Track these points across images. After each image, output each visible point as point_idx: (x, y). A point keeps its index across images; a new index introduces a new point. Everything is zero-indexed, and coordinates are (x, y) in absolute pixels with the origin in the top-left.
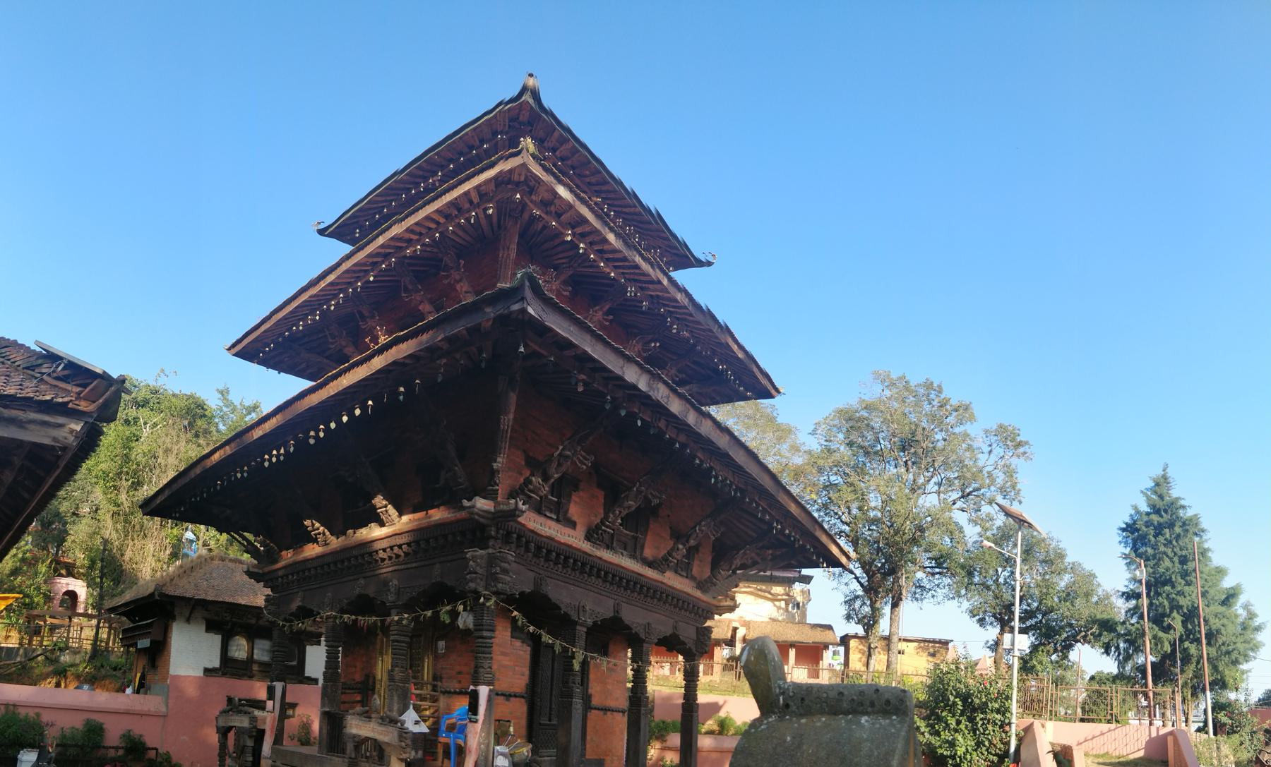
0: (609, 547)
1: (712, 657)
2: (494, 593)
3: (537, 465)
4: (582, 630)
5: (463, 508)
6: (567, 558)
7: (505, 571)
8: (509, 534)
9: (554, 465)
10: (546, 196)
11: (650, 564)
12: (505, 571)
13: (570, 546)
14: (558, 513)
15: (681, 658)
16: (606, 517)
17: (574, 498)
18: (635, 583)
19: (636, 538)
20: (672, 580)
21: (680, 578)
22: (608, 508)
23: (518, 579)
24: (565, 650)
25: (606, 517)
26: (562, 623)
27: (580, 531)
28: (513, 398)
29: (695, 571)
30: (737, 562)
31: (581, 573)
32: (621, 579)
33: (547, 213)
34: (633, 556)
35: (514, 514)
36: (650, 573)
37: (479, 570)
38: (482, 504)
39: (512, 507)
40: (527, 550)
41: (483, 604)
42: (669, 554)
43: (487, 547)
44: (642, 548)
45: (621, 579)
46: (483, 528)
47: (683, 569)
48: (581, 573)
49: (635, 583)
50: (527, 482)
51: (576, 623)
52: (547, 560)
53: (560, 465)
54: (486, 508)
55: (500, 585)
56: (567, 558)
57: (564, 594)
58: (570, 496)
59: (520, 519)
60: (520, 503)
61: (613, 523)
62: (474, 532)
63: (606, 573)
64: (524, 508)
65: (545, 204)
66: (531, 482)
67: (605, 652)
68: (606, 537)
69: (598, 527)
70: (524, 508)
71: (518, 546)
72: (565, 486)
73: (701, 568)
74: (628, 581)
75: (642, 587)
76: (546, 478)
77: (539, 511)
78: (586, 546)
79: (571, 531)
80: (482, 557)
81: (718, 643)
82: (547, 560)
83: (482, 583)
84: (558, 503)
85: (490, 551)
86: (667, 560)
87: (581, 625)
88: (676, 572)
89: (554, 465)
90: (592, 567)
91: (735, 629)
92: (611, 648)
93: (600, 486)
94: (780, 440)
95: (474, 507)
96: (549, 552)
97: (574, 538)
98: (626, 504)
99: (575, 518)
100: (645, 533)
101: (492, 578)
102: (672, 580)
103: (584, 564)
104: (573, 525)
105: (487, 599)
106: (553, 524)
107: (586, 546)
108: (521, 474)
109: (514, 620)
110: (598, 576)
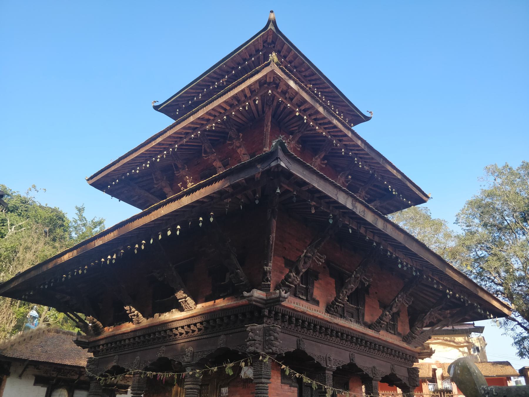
0: (342, 316)
1: (421, 390)
2: (268, 353)
3: (291, 264)
4: (329, 373)
5: (244, 297)
6: (315, 325)
7: (276, 339)
8: (276, 314)
9: (302, 263)
10: (285, 88)
11: (370, 327)
12: (276, 339)
13: (316, 317)
14: (307, 296)
15: (399, 391)
16: (338, 296)
17: (316, 284)
18: (362, 340)
19: (358, 310)
20: (384, 336)
21: (390, 335)
22: (339, 290)
23: (285, 343)
24: (320, 387)
25: (338, 296)
26: (315, 369)
27: (322, 307)
28: (274, 223)
29: (400, 329)
30: (427, 321)
31: (326, 335)
32: (352, 337)
33: (286, 99)
34: (358, 322)
35: (278, 300)
36: (370, 332)
37: (257, 338)
38: (258, 294)
39: (278, 295)
40: (290, 322)
41: (262, 361)
42: (381, 318)
43: (263, 323)
45: (352, 337)
46: (260, 310)
47: (392, 328)
48: (326, 335)
49: (362, 340)
50: (288, 277)
51: (324, 369)
52: (303, 327)
53: (305, 263)
54: (262, 296)
56: (315, 325)
57: (316, 350)
58: (313, 283)
59: (283, 303)
60: (283, 293)
61: (343, 300)
62: (254, 313)
63: (342, 334)
64: (286, 295)
65: (284, 93)
66: (290, 277)
67: (346, 387)
68: (339, 309)
70: (286, 295)
71: (283, 322)
72: (310, 278)
73: (403, 327)
74: (357, 339)
75: (366, 342)
76: (297, 273)
77: (295, 295)
78: (327, 317)
79: (315, 307)
80: (259, 330)
81: (424, 380)
82: (303, 327)
83: (261, 347)
84: (307, 289)
85: (265, 325)
86: (380, 323)
87: (328, 370)
88: (387, 331)
89: (302, 263)
90: (332, 331)
91: (434, 370)
92: (351, 385)
93: (332, 275)
94: (437, 231)
95: (252, 296)
96: (303, 322)
97: (318, 312)
98: (349, 286)
99: (318, 298)
101: (267, 343)
102: (384, 336)
103: (327, 329)
104: (317, 303)
105: (264, 357)
106: (304, 303)
107: (327, 317)
108: (281, 272)
109: (283, 371)
110: (337, 336)
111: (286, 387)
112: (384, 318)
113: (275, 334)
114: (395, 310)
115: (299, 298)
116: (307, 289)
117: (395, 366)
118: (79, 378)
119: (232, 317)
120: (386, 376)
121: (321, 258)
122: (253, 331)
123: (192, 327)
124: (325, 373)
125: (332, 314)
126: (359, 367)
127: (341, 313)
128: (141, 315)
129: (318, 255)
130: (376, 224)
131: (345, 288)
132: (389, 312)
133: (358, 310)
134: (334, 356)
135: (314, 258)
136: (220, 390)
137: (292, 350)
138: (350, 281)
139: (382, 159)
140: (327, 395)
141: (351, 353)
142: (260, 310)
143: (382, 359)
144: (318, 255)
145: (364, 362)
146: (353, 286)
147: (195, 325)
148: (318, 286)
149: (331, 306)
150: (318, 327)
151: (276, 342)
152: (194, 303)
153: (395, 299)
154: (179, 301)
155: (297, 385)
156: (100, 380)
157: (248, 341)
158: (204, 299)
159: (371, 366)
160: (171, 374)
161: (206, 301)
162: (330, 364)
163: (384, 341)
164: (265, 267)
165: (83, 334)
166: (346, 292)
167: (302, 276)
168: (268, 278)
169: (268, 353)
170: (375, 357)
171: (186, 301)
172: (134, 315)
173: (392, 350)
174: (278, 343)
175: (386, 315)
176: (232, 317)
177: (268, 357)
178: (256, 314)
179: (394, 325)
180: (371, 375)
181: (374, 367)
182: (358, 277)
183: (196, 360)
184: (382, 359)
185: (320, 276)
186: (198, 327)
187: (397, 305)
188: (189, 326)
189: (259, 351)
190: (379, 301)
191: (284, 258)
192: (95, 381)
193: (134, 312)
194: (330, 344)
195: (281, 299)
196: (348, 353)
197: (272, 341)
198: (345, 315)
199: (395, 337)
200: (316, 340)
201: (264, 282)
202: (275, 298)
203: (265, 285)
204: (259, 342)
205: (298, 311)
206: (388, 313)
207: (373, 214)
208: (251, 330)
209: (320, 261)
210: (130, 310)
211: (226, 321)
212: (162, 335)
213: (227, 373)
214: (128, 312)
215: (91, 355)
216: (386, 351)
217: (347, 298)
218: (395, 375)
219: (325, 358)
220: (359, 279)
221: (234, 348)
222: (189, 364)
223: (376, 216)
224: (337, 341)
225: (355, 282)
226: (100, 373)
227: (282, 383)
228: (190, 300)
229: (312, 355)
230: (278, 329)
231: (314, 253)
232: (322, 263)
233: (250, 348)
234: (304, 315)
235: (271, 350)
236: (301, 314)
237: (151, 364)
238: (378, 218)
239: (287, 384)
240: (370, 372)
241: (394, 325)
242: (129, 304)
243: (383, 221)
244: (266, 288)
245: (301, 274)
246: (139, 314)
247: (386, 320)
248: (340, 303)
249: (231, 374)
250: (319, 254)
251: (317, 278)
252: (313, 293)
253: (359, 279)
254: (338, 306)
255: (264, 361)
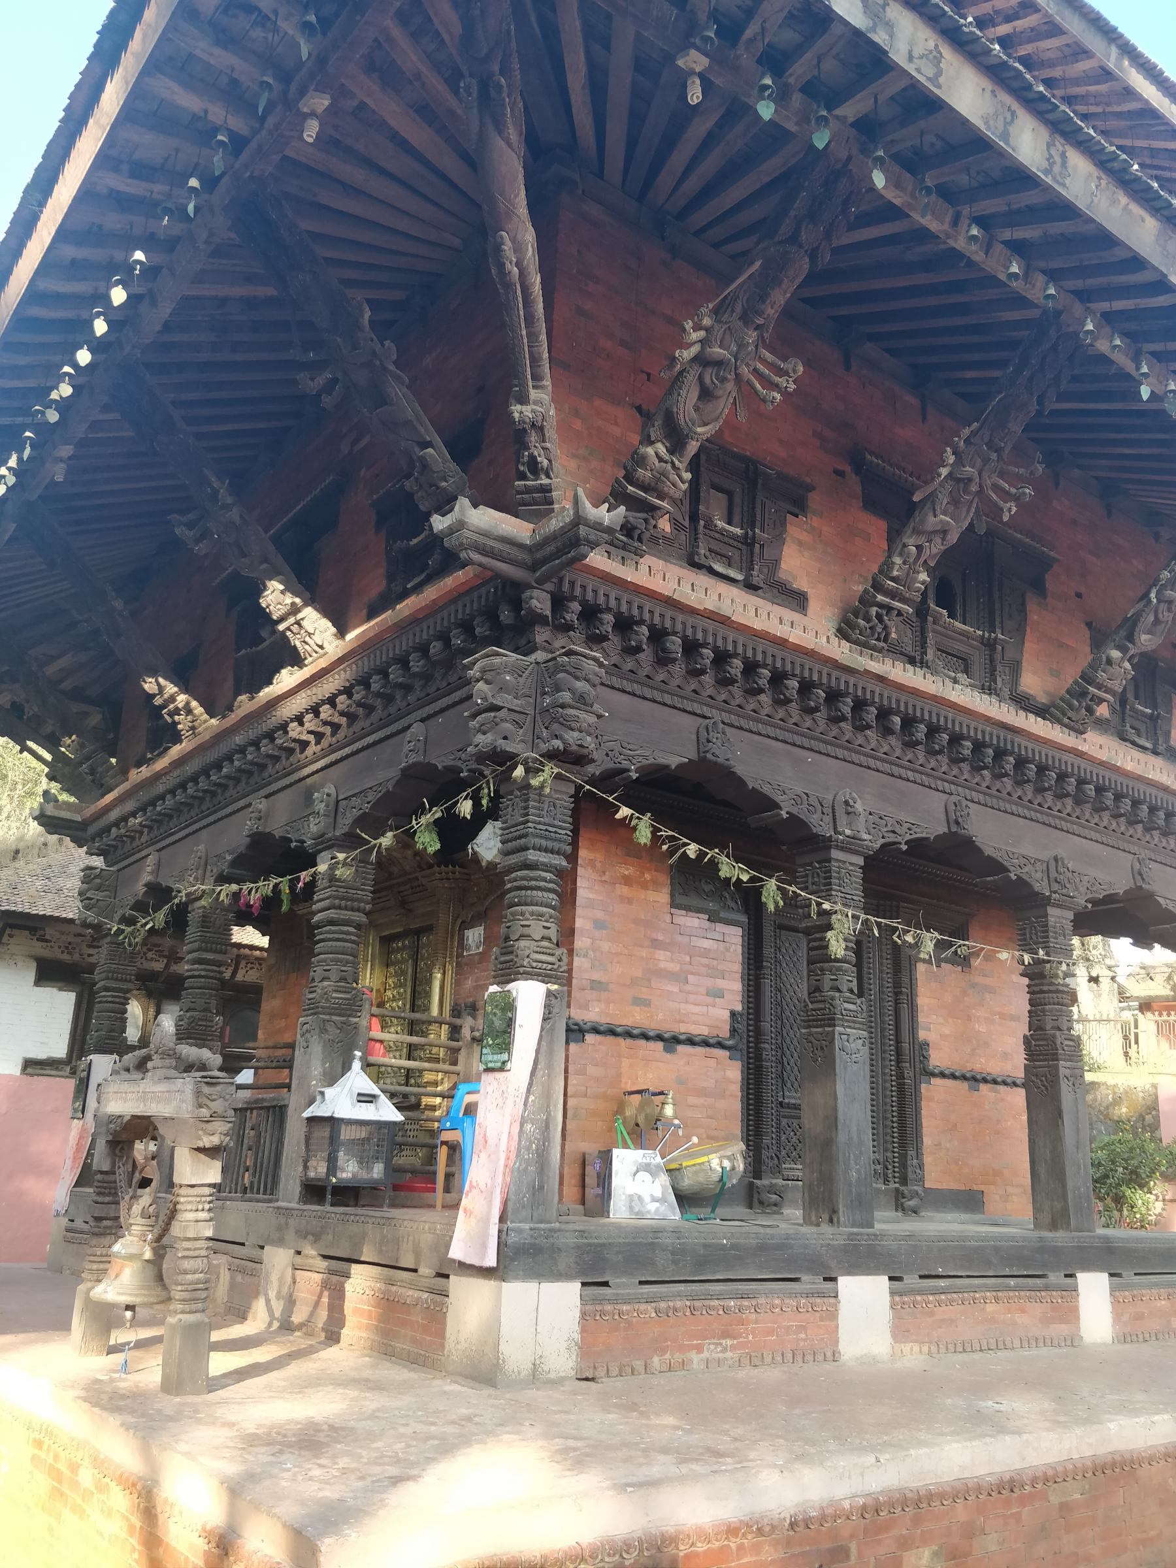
2: (552, 755)
7: (582, 701)
9: (689, 395)
11: (1042, 712)
12: (582, 701)
13: (782, 643)
17: (795, 530)
21: (1136, 753)
26: (786, 844)
34: (989, 689)
38: (484, 519)
42: (1087, 678)
43: (534, 649)
44: (1015, 669)
46: (513, 592)
49: (1000, 754)
53: (706, 394)
55: (572, 737)
57: (784, 771)
61: (906, 581)
62: (500, 612)
66: (641, 461)
69: (866, 600)
75: (1021, 763)
76: (677, 443)
78: (841, 651)
79: (789, 615)
80: (518, 672)
84: (748, 542)
85: (540, 656)
86: (1084, 694)
87: (842, 849)
89: (689, 395)
95: (461, 525)
99: (801, 583)
100: (1020, 631)
104: (797, 600)
107: (841, 651)
111: (693, 922)
112: (1101, 676)
113: (580, 685)
114: (1146, 640)
115: (712, 572)
116: (748, 542)
117: (1152, 865)
118: (167, 966)
119: (436, 647)
120: (1110, 898)
121: (782, 373)
122: (488, 676)
123: (326, 712)
124: (829, 860)
125: (865, 645)
126: (988, 851)
127: (909, 649)
128: (201, 710)
129: (763, 361)
130: (1005, 136)
131: (917, 532)
132: (1123, 649)
133: (990, 645)
134: (869, 803)
135: (744, 370)
136: (462, 939)
137: (674, 761)
138: (931, 498)
139: (1114, 51)
140: (829, 934)
141: (954, 798)
142: (513, 592)
143: (1094, 835)
144: (763, 361)
145: (1009, 836)
146: (945, 523)
147: (331, 701)
148: (805, 537)
149: (856, 614)
150: (794, 684)
151: (582, 715)
152: (334, 630)
153: (1146, 596)
154: (281, 627)
155: (744, 919)
156: (120, 932)
157: (474, 716)
158: (365, 612)
159: (1046, 855)
160: (274, 880)
161: (370, 617)
162: (850, 824)
163: (1102, 764)
164: (516, 410)
165: (64, 797)
166: (919, 548)
167: (697, 456)
168: (533, 458)
169: (552, 755)
170: (1064, 825)
171: (298, 623)
172: (177, 711)
173: (1136, 803)
174: (592, 719)
175: (1109, 662)
176: (436, 647)
177: (550, 769)
178: (506, 615)
179: (1154, 719)
180: (1041, 886)
181: (1056, 859)
182: (970, 480)
183: (345, 824)
184: (1094, 835)
185: (814, 499)
186: (340, 707)
187: (1157, 622)
188: (315, 710)
189: (510, 747)
190: (1089, 625)
191: (639, 409)
192: (108, 939)
193: (172, 699)
194: (855, 757)
195: (583, 531)
196: (935, 803)
197: (563, 706)
198: (930, 655)
199: (1158, 761)
200: (788, 736)
201: (523, 477)
202: (564, 531)
203: (528, 490)
204: (517, 717)
205: (693, 611)
206: (1116, 654)
207: (987, 84)
208: (483, 671)
209: (776, 387)
210: (161, 689)
211: (416, 665)
212: (249, 757)
213: (420, 846)
214: (158, 701)
215: (98, 862)
216: (1109, 803)
217: (923, 576)
218: (1150, 896)
219: (827, 803)
220: (974, 488)
221: (449, 762)
222: (325, 843)
223: (1007, 99)
224: (886, 748)
225: (955, 502)
226: (120, 913)
227: (674, 904)
228: (312, 618)
229: (766, 789)
230: (591, 666)
231: (741, 346)
232: (784, 392)
233: (480, 739)
234: (722, 631)
235: (557, 743)
236: (710, 626)
237: (234, 864)
238: (1016, 106)
239: (699, 911)
240: (1038, 875)
241: (1154, 719)
242: (154, 673)
243: (1044, 133)
244: (535, 504)
245: (693, 447)
246: (194, 704)
247: (1109, 684)
248: (893, 595)
249: (431, 850)
250: (769, 357)
251: (798, 505)
252: (776, 563)
253: (974, 488)
254: (890, 609)
255: (535, 782)
